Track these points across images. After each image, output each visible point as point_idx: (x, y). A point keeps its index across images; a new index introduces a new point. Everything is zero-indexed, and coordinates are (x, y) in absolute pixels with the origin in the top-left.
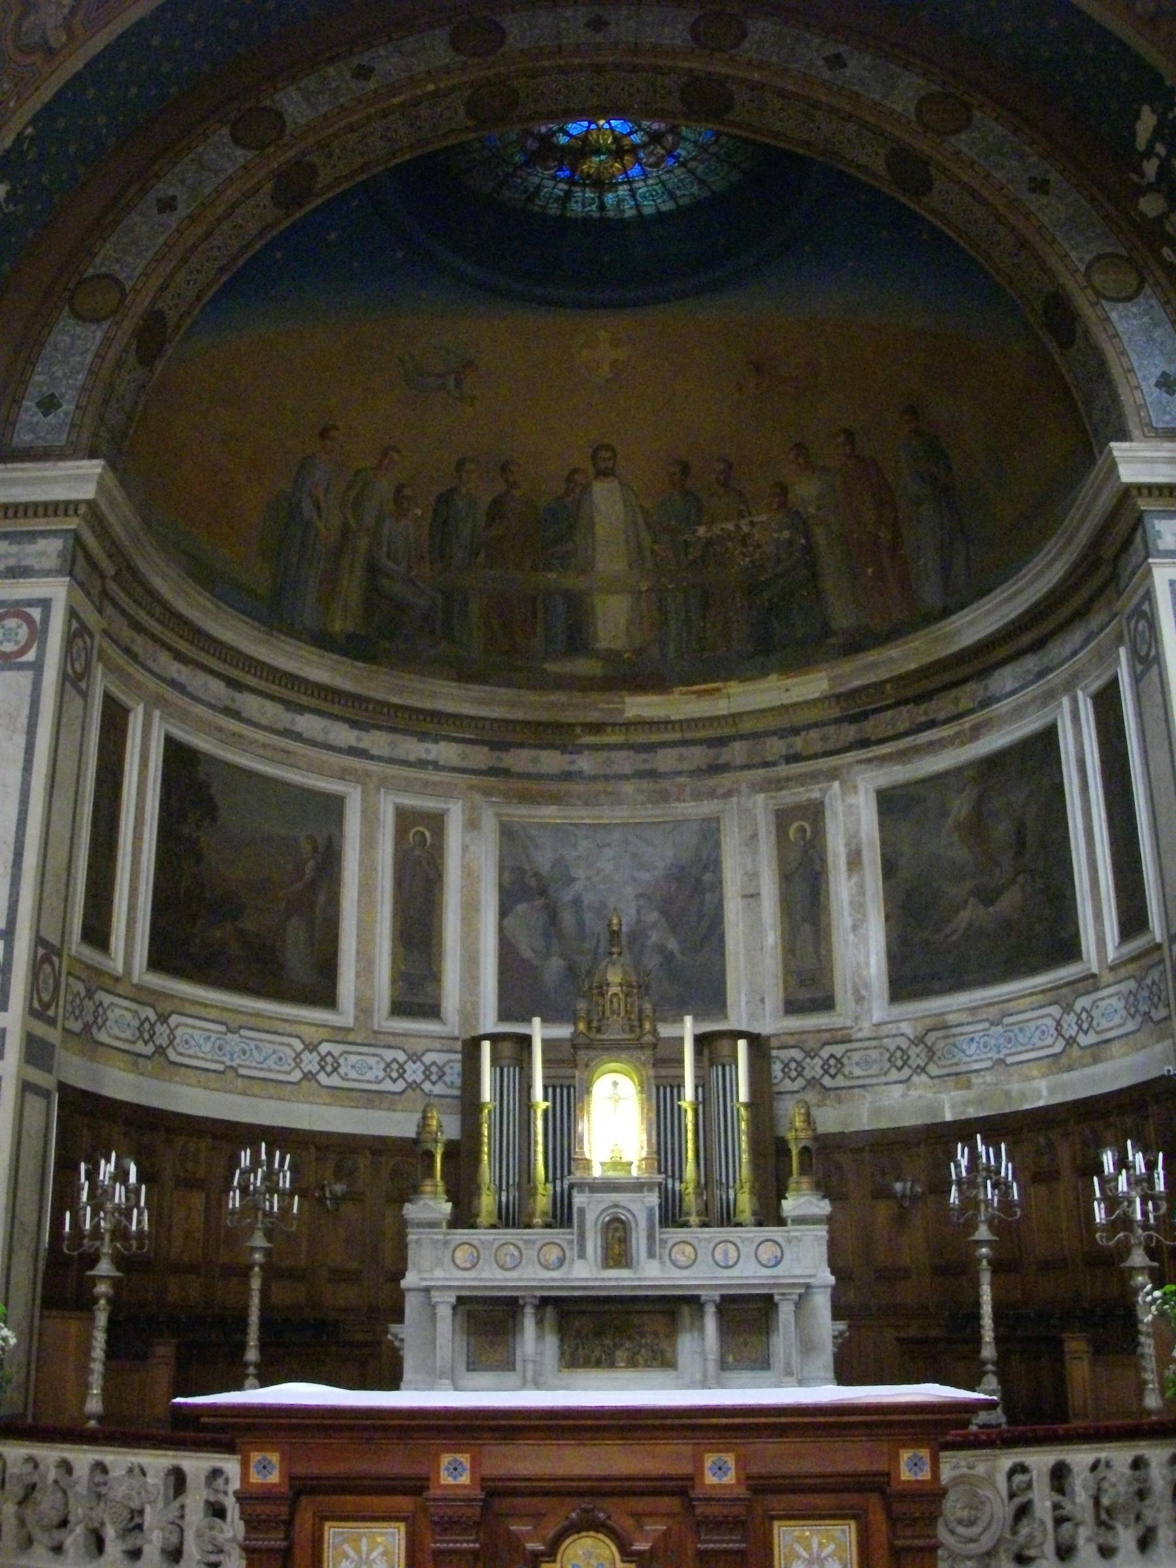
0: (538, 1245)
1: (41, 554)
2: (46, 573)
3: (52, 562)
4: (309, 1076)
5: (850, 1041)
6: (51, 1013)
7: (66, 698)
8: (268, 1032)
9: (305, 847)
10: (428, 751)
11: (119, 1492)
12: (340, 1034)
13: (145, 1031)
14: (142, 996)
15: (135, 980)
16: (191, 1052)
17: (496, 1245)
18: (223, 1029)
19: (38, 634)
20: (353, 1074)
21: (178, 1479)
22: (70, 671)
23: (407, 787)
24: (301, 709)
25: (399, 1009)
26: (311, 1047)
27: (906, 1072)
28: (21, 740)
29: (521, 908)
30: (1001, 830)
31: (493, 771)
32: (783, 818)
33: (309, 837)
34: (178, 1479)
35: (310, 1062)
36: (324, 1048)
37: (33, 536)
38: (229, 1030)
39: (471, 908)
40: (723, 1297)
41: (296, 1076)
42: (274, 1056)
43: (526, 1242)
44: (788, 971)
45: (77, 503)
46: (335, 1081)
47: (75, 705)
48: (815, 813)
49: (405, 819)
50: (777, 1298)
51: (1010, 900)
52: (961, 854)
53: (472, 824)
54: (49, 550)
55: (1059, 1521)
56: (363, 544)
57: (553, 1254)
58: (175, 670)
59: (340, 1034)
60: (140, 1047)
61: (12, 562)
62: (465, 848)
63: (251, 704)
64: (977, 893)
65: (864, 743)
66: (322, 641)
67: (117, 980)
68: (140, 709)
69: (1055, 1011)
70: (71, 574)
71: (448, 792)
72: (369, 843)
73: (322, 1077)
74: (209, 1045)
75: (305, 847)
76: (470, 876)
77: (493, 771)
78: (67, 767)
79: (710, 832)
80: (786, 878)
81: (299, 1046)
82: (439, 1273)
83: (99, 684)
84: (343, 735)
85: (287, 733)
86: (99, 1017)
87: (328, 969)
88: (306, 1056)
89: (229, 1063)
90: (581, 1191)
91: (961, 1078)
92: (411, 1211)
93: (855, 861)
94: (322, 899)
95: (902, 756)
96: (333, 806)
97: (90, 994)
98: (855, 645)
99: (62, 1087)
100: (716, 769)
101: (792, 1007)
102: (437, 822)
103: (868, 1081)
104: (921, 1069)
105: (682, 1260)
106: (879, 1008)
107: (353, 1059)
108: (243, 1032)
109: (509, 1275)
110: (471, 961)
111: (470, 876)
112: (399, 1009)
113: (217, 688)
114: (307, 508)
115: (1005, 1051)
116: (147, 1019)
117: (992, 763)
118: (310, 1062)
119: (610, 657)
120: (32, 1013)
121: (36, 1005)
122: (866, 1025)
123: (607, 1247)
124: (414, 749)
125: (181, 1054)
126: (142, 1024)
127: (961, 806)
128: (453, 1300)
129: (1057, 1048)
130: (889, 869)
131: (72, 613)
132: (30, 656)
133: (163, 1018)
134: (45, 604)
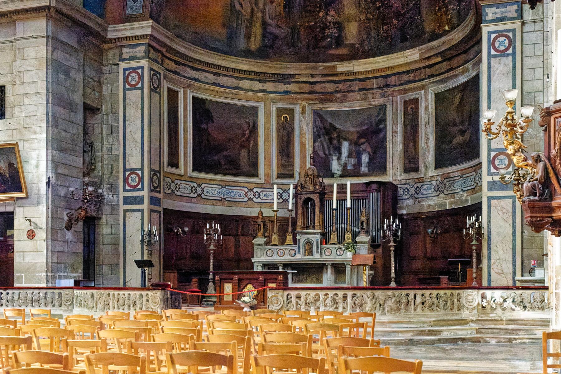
0: (289, 249)
1: (140, 52)
2: (142, 58)
3: (143, 54)
4: (251, 199)
5: (423, 182)
6: (158, 189)
7: (152, 97)
8: (236, 187)
9: (245, 126)
10: (287, 87)
11: (132, 299)
12: (261, 186)
13: (195, 190)
14: (192, 179)
15: (189, 175)
16: (210, 195)
17: (278, 250)
18: (220, 187)
19: (141, 78)
20: (265, 198)
21: (141, 295)
22: (152, 87)
23: (281, 101)
24: (242, 79)
26: (251, 190)
27: (439, 192)
28: (140, 111)
31: (311, 92)
32: (406, 103)
33: (246, 122)
34: (141, 295)
35: (251, 195)
36: (255, 190)
37: (136, 46)
38: (222, 187)
40: (332, 264)
41: (246, 199)
42: (238, 194)
43: (285, 249)
44: (406, 158)
45: (147, 35)
46: (259, 200)
47: (156, 97)
48: (416, 101)
49: (280, 112)
50: (346, 264)
53: (303, 112)
54: (141, 50)
55: (297, 304)
56: (259, 15)
57: (292, 252)
58: (194, 74)
59: (261, 186)
60: (192, 195)
61: (131, 54)
63: (222, 80)
66: (248, 54)
67: (182, 176)
68: (182, 90)
69: (474, 173)
70: (149, 58)
71: (293, 101)
73: (254, 199)
74: (216, 192)
75: (245, 126)
77: (311, 92)
78: (155, 118)
79: (382, 108)
81: (246, 190)
82: (262, 258)
83: (166, 85)
84: (257, 85)
86: (178, 188)
87: (255, 165)
88: (249, 193)
89: (223, 197)
90: (299, 235)
91: (453, 194)
92: (255, 241)
94: (252, 142)
95: (443, 81)
96: (255, 110)
97: (173, 181)
98: (434, 36)
99: (164, 209)
100: (387, 86)
101: (407, 170)
102: (291, 112)
103: (428, 195)
104: (442, 192)
105: (327, 254)
106: (432, 172)
107: (264, 193)
108: (227, 187)
109: (281, 258)
113: (211, 77)
115: (463, 187)
116: (194, 186)
117: (465, 84)
118: (251, 195)
119: (352, 46)
120: (151, 190)
121: (152, 188)
122: (427, 176)
124: (282, 87)
125: (206, 196)
126: (192, 188)
128: (262, 265)
129: (474, 186)
131: (151, 69)
132: (140, 85)
133: (200, 186)
134: (142, 68)
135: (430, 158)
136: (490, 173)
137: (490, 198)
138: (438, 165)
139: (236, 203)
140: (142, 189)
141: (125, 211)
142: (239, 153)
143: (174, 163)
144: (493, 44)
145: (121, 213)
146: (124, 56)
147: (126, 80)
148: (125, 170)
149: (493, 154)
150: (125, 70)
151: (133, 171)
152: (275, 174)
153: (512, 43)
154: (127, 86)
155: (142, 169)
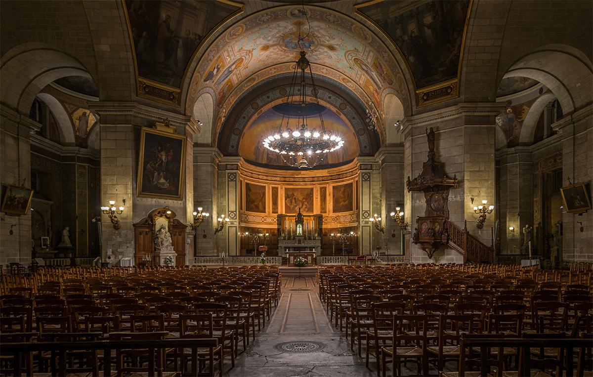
1: (234, 167)
4: (263, 221)
24: (260, 175)
25: (273, 213)
29: (288, 199)
30: (346, 193)
31: (284, 181)
32: (321, 188)
34: (273, 258)
39: (282, 199)
51: (347, 202)
52: (342, 195)
53: (282, 188)
62: (281, 192)
64: (343, 201)
65: (332, 180)
72: (269, 192)
76: (281, 195)
79: (312, 189)
80: (321, 196)
85: (258, 178)
87: (265, 208)
91: (340, 223)
93: (330, 195)
95: (336, 182)
110: (282, 206)
111: (281, 195)
112: (273, 213)
114: (260, 147)
123: (298, 242)
127: (342, 190)
130: (334, 196)
135: (331, 208)
136: (362, 218)
137: (362, 226)
138: (334, 212)
139: (259, 223)
140: (236, 219)
141: (229, 227)
142: (259, 204)
143: (241, 209)
144: (363, 177)
145: (227, 227)
146: (228, 168)
147: (229, 177)
148: (229, 211)
149: (363, 212)
150: (228, 173)
151: (232, 212)
152: (271, 212)
153: (369, 177)
154: (229, 180)
155: (236, 211)
